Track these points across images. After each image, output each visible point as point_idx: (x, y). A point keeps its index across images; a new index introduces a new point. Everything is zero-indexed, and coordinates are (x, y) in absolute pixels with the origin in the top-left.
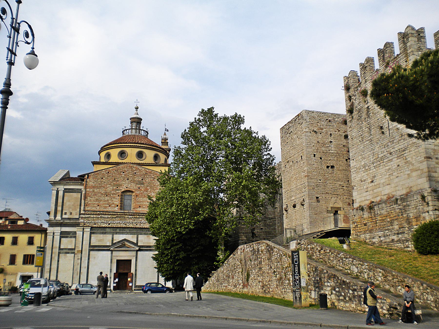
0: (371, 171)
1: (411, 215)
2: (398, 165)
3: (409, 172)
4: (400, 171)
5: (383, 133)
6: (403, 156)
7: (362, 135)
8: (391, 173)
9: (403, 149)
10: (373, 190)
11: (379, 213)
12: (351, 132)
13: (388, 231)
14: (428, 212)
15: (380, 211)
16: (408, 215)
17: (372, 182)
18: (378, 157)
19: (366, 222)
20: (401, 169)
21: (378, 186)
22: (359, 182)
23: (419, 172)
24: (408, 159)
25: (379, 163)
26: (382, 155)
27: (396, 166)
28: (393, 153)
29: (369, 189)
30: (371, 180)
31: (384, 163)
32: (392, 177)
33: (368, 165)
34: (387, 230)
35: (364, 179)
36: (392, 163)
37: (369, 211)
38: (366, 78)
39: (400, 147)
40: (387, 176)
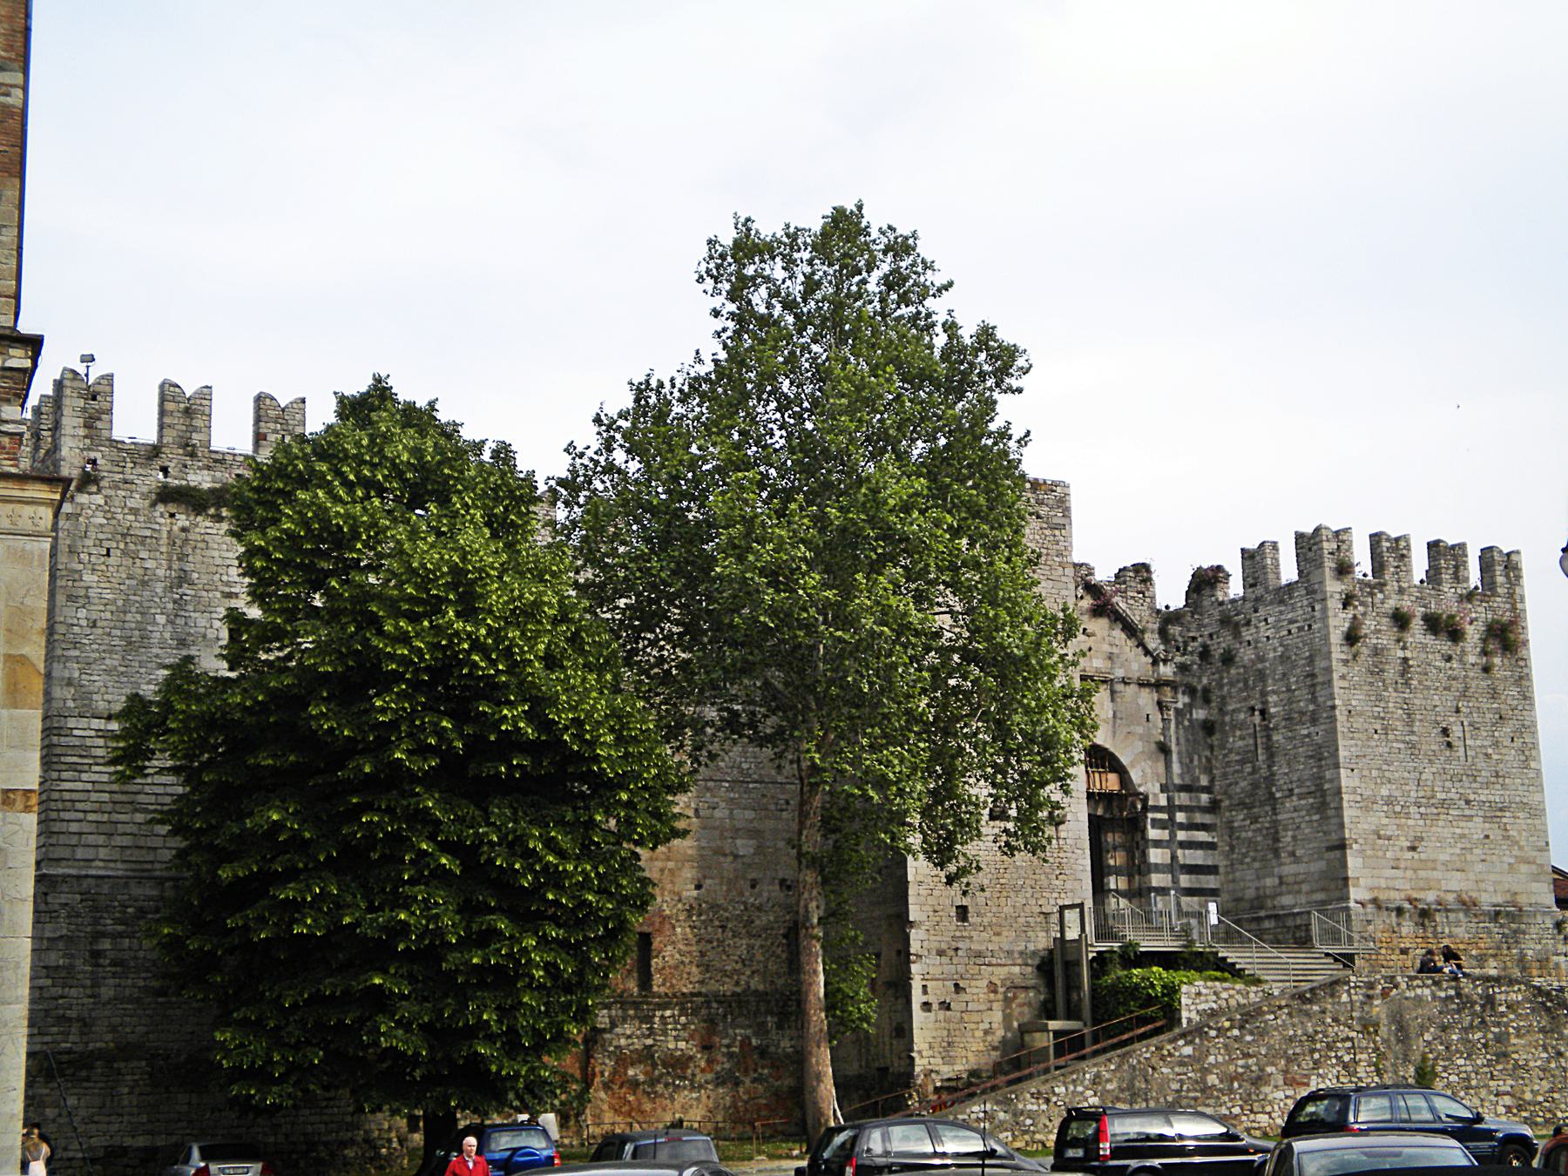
0: (1410, 822)
1: (1530, 953)
2: (1487, 837)
3: (1512, 861)
5: (1449, 745)
7: (1383, 719)
8: (1469, 846)
10: (1415, 870)
11: (1447, 930)
15: (1450, 927)
17: (1413, 849)
19: (1408, 945)
21: (1430, 865)
23: (1534, 867)
24: (1511, 833)
25: (1435, 811)
26: (1443, 796)
29: (1402, 864)
30: (1409, 844)
32: (1469, 857)
35: (1388, 833)
36: (1470, 824)
37: (1416, 918)
39: (1492, 798)
40: (1458, 851)
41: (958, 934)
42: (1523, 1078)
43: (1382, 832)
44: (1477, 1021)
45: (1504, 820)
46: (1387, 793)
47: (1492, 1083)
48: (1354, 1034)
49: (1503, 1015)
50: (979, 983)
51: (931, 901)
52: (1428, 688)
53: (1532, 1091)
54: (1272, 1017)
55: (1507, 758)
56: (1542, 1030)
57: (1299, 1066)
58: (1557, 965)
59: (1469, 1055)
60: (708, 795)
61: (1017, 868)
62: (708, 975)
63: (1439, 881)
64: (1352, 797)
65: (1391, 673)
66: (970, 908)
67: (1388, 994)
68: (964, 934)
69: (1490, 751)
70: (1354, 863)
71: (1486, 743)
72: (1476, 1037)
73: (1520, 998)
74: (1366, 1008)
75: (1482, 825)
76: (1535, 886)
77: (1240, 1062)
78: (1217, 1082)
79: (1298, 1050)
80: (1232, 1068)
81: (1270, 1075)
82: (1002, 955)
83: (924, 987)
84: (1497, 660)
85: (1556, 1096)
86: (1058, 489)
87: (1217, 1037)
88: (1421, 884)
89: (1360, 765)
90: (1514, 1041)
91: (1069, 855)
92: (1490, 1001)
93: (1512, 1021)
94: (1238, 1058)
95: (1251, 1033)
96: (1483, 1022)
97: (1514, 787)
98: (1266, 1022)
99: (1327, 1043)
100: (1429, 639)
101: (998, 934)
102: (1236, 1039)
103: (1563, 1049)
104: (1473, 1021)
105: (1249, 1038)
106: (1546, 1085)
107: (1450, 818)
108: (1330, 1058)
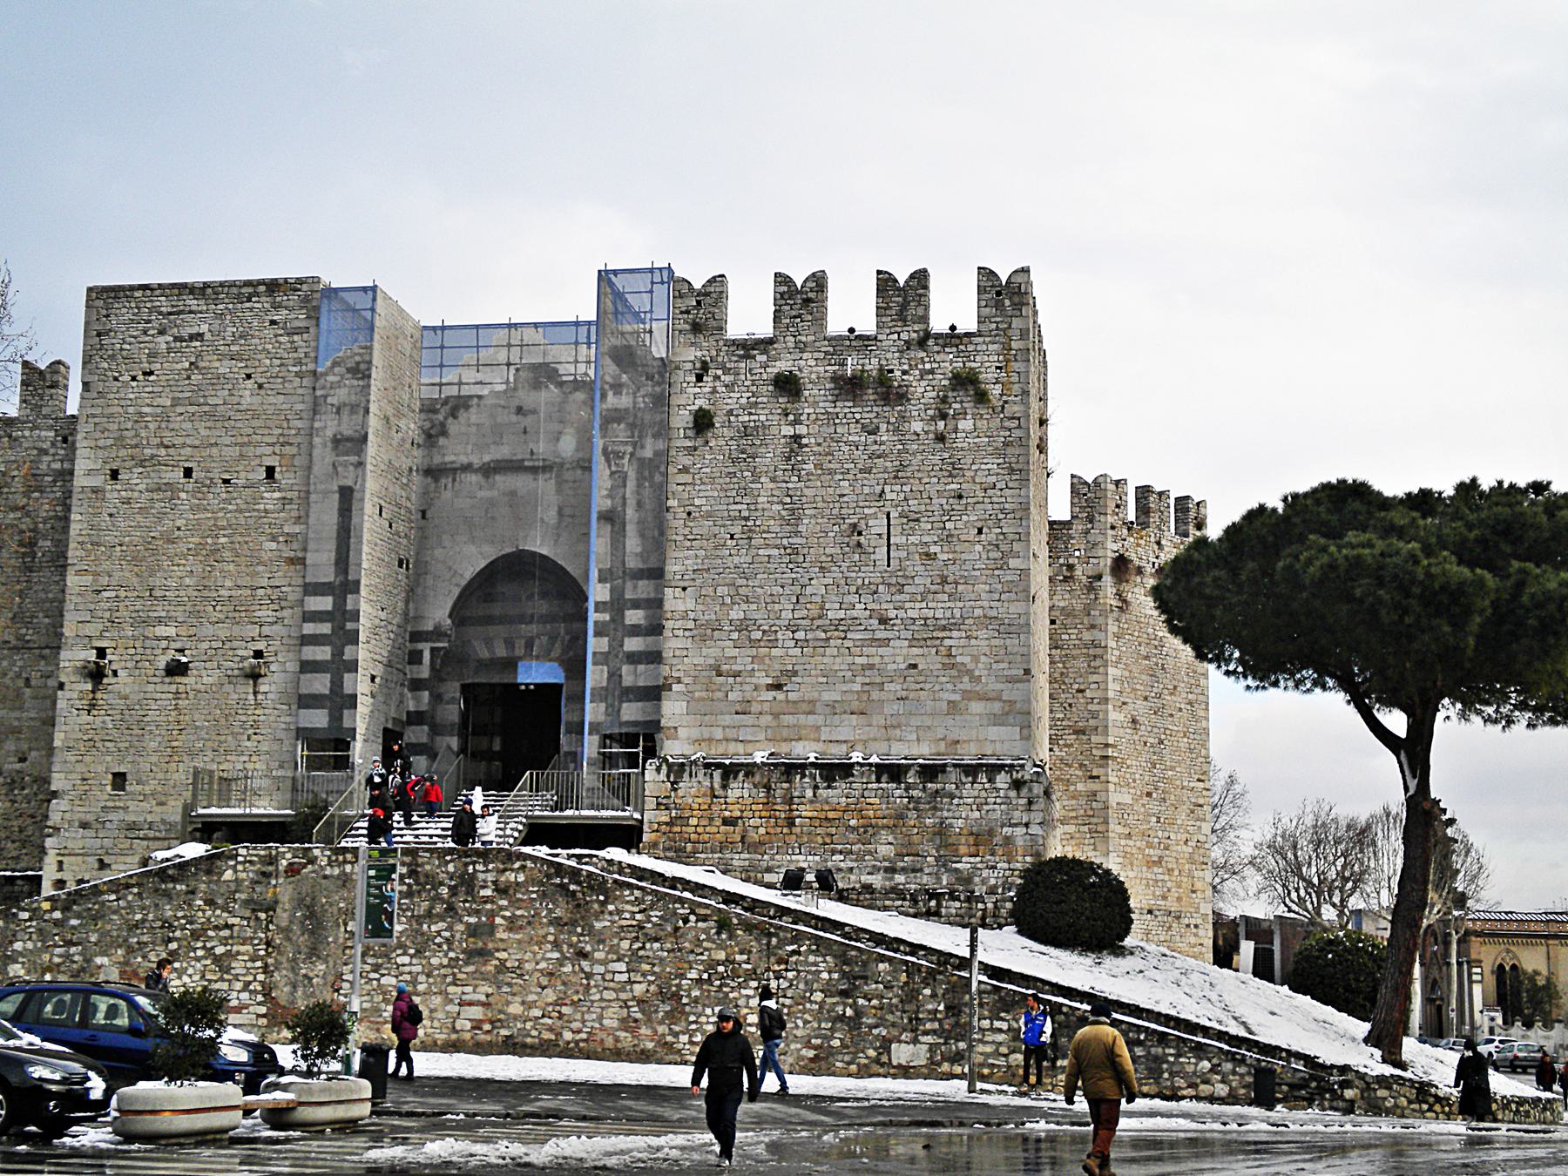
0: (774, 652)
2: (915, 666)
3: (957, 697)
4: (919, 686)
6: (938, 642)
7: (746, 519)
8: (878, 680)
9: (944, 622)
10: (776, 716)
12: (688, 488)
13: (842, 857)
14: (1027, 825)
16: (942, 823)
17: (778, 687)
18: (820, 617)
20: (922, 679)
21: (805, 707)
22: (704, 673)
24: (959, 659)
25: (823, 635)
26: (841, 614)
27: (903, 666)
28: (899, 622)
29: (755, 708)
31: (848, 643)
32: (875, 695)
33: (766, 628)
34: (841, 853)
35: (734, 667)
38: (804, 339)
40: (857, 687)
41: (110, 804)
42: (509, 985)
43: (725, 667)
44: (438, 909)
45: (947, 642)
46: (742, 615)
47: (451, 989)
48: (236, 921)
49: (487, 900)
50: (128, 859)
51: (79, 768)
52: (832, 472)
53: (523, 1003)
54: (113, 897)
55: (964, 556)
56: (556, 922)
57: (144, 957)
58: (1008, 840)
59: (418, 951)
60: (43, 663)
61: (197, 728)
62: (24, 851)
63: (818, 728)
64: (679, 624)
65: (769, 457)
66: (129, 777)
67: (298, 872)
68: (118, 804)
69: (934, 549)
70: (672, 709)
71: (926, 539)
72: (434, 928)
73: (521, 878)
74: (258, 889)
75: (905, 651)
76: (994, 732)
77: (58, 951)
78: (22, 972)
79: (145, 939)
80: (46, 957)
81: (100, 967)
82: (162, 827)
83: (60, 863)
84: (965, 424)
85: (565, 1010)
86: (305, 287)
87: (30, 919)
88: (785, 733)
89: (698, 582)
90: (501, 935)
91: (267, 712)
92: (467, 883)
93: (502, 908)
94: (56, 946)
95: (79, 916)
96: (451, 908)
97: (973, 596)
98: (103, 903)
99: (193, 932)
100: (844, 407)
101: (162, 804)
102: (56, 923)
103: (588, 948)
104: (432, 908)
105: (74, 922)
106: (549, 995)
107: (848, 643)
108: (195, 949)
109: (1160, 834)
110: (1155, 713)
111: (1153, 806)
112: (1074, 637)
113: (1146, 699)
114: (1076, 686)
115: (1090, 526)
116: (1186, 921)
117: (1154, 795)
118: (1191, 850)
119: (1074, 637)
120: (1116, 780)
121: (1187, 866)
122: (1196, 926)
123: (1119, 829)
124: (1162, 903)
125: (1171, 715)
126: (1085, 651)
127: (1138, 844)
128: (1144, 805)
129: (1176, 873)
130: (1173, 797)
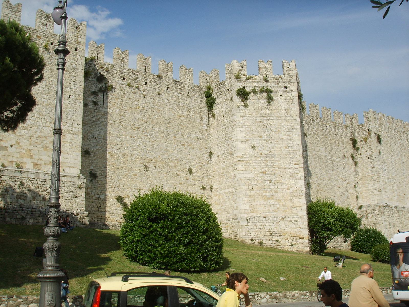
109: (272, 187)
110: (266, 141)
111: (267, 177)
112: (228, 120)
113: (261, 137)
114: (229, 138)
115: (230, 80)
116: (289, 219)
117: (267, 173)
118: (291, 191)
119: (228, 120)
120: (244, 169)
121: (289, 198)
122: (296, 221)
123: (247, 187)
124: (275, 213)
125: (277, 141)
126: (231, 124)
127: (258, 192)
128: (261, 177)
129: (283, 201)
130: (280, 172)
